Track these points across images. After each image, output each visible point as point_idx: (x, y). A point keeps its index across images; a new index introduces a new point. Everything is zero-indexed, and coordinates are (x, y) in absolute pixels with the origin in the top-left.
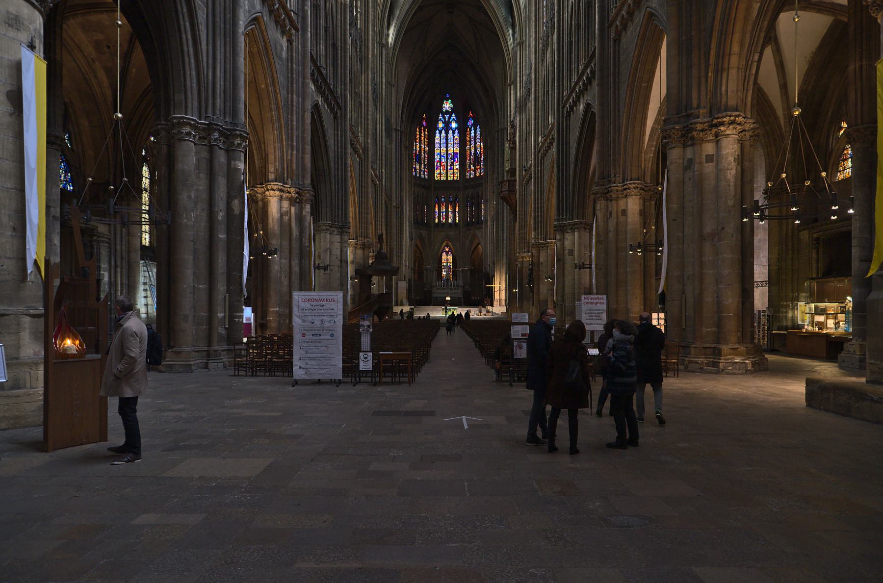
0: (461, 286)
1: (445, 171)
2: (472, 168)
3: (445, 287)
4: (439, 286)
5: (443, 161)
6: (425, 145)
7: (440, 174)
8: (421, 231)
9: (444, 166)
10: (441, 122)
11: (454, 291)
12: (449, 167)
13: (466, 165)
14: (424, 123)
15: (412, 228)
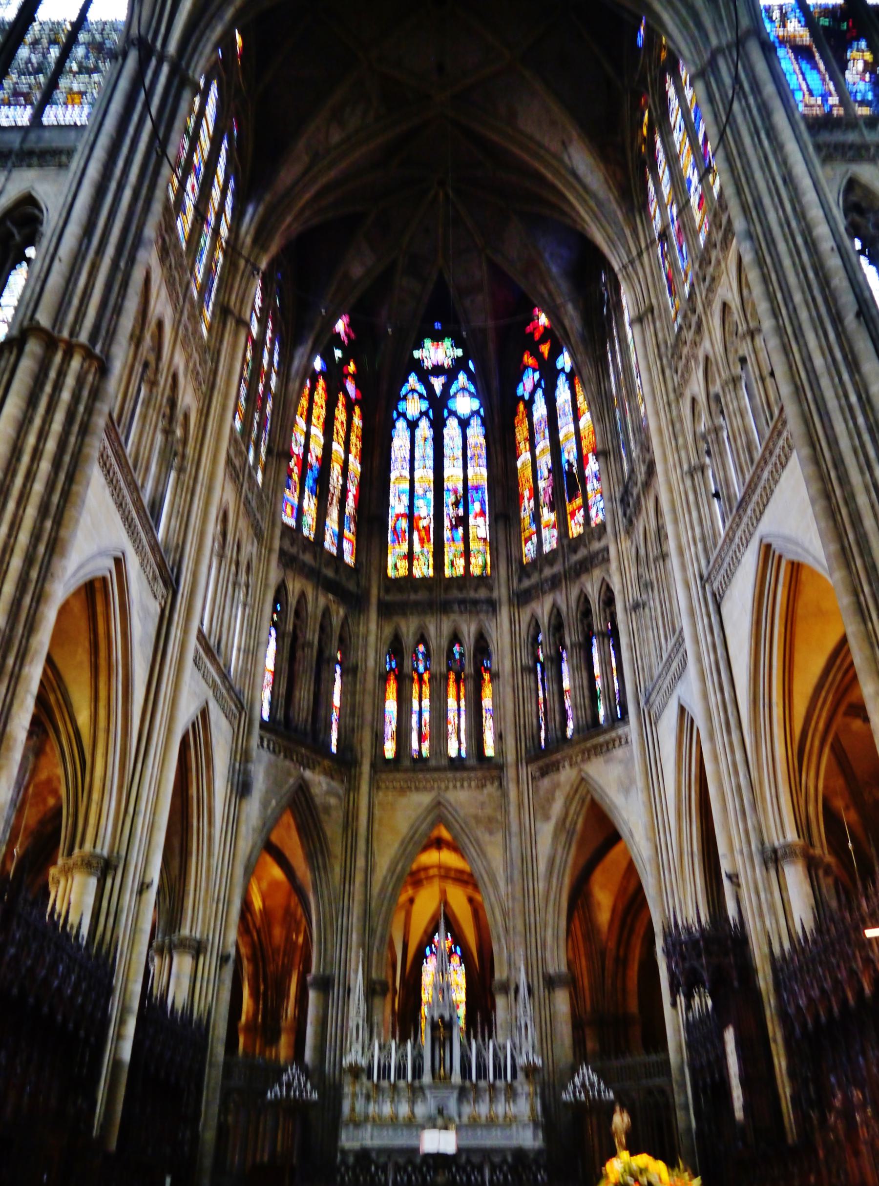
0: (531, 1071)
1: (430, 547)
2: (548, 516)
3: (427, 1078)
4: (384, 1071)
5: (423, 513)
6: (347, 451)
7: (410, 556)
8: (308, 774)
9: (426, 528)
10: (416, 396)
11: (483, 1109)
12: (447, 534)
13: (519, 520)
14: (351, 387)
15: (249, 732)
